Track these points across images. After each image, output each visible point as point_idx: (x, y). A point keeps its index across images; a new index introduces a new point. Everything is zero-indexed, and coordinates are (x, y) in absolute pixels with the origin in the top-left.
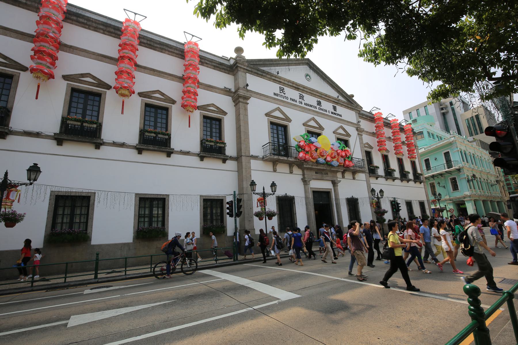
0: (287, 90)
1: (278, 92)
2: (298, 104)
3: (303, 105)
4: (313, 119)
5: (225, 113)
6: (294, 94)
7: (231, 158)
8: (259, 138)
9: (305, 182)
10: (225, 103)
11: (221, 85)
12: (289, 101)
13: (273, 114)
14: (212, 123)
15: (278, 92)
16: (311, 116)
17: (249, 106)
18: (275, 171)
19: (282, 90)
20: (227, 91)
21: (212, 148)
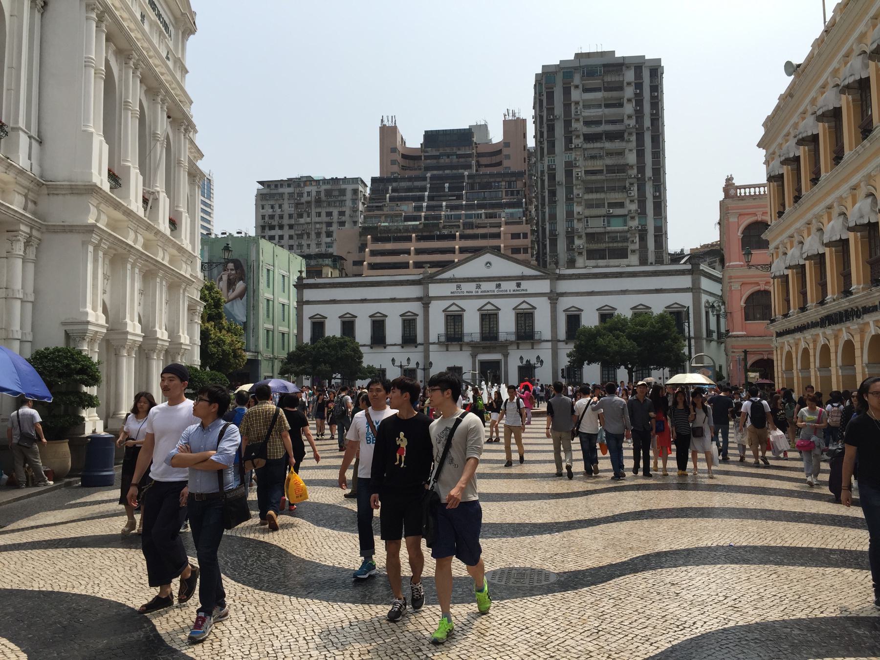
0: (462, 284)
1: (455, 290)
2: (474, 294)
3: (480, 294)
4: (489, 303)
5: (417, 315)
6: (470, 287)
7: (420, 344)
8: (438, 327)
9: (474, 356)
10: (415, 307)
11: (414, 296)
12: (465, 294)
13: (449, 309)
14: (409, 323)
15: (455, 290)
16: (485, 301)
17: (431, 309)
18: (447, 350)
19: (459, 287)
20: (418, 299)
21: (409, 340)
